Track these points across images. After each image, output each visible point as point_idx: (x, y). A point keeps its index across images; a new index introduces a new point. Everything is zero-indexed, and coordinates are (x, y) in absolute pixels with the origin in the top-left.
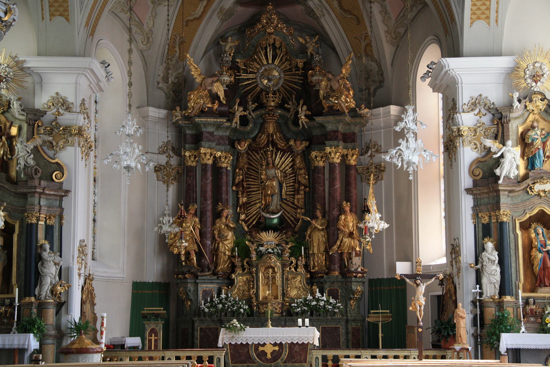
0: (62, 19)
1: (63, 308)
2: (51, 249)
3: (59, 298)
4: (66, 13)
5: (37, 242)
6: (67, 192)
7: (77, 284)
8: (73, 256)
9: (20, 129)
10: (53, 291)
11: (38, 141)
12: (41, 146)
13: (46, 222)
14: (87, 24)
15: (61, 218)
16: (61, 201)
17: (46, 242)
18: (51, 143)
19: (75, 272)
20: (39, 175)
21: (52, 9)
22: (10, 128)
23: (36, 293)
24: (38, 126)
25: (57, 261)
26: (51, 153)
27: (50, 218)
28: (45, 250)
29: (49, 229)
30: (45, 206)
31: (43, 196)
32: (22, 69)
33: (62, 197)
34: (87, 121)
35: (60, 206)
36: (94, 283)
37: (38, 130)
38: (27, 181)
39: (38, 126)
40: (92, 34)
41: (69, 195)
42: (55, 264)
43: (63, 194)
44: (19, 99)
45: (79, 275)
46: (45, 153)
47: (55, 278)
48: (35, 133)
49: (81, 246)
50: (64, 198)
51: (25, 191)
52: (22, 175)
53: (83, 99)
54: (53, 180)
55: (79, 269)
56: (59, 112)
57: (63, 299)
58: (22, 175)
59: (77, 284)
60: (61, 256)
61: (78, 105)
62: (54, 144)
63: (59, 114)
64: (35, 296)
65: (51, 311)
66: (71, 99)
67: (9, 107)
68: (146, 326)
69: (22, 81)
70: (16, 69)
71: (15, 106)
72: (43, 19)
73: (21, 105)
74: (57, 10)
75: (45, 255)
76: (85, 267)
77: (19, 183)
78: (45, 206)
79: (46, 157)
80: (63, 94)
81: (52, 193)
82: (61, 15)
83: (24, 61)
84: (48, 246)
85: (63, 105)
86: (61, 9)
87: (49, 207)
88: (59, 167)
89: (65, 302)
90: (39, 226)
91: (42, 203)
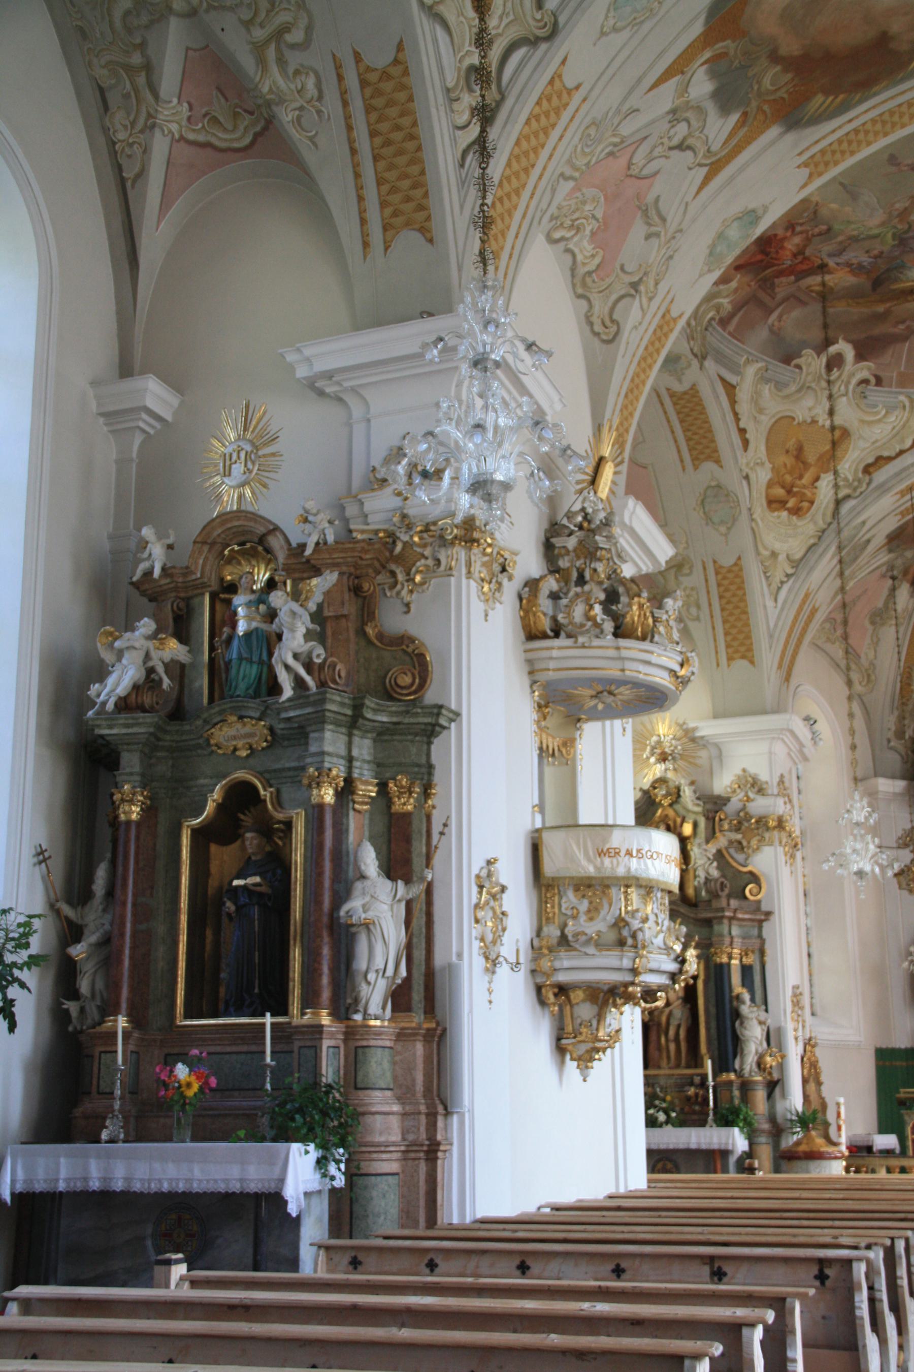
0: (745, 663)
1: (777, 1091)
2: (753, 1000)
3: (770, 1074)
4: (749, 654)
5: (731, 990)
6: (768, 914)
7: (794, 1052)
8: (785, 1011)
9: (695, 825)
10: (760, 1064)
11: (721, 841)
12: (727, 848)
14: (780, 666)
15: (762, 953)
16: (760, 928)
18: (740, 843)
19: (790, 1035)
20: (727, 891)
21: (730, 651)
22: (681, 825)
23: (737, 1066)
24: (721, 820)
25: (762, 1018)
26: (740, 857)
27: (747, 954)
28: (743, 1003)
29: (746, 970)
30: (738, 936)
31: (734, 922)
32: (693, 740)
33: (760, 922)
34: (788, 806)
35: (760, 936)
36: (818, 1051)
37: (721, 826)
38: (709, 901)
39: (721, 820)
40: (787, 679)
41: (772, 918)
42: (761, 1023)
43: (763, 917)
44: (692, 783)
45: (796, 1039)
47: (761, 1044)
48: (717, 830)
49: (795, 995)
50: (765, 924)
51: (709, 915)
52: (703, 893)
53: (782, 776)
54: (745, 898)
55: (796, 1030)
56: (748, 798)
57: (776, 1076)
58: (703, 893)
59: (794, 1052)
60: (766, 1011)
61: (775, 784)
62: (745, 843)
63: (749, 800)
64: (735, 1071)
65: (760, 1095)
66: (764, 776)
67: (679, 796)
68: (906, 1118)
69: (694, 757)
70: (685, 740)
71: (687, 793)
72: (718, 665)
73: (695, 792)
74: (737, 651)
75: (745, 1009)
76: (803, 1027)
78: (738, 936)
79: (734, 864)
80: (752, 770)
81: (747, 916)
82: (743, 657)
83: (695, 729)
84: (747, 997)
85: (753, 786)
86: (743, 649)
87: (744, 938)
88: (754, 878)
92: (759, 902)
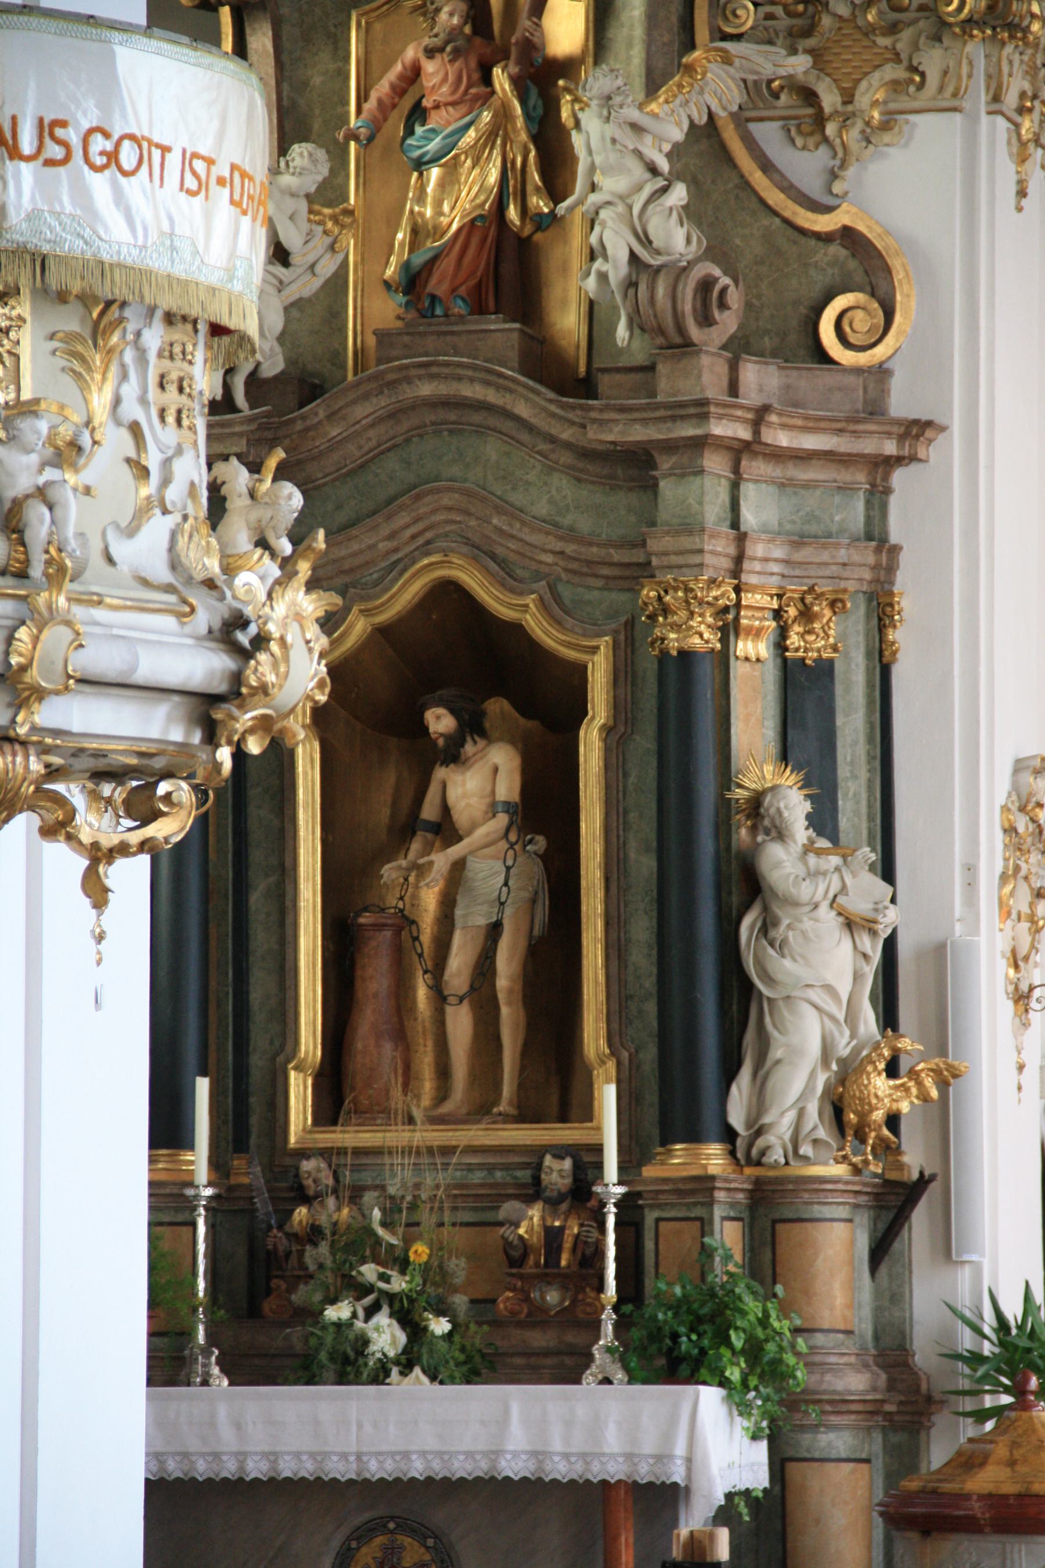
1: (920, 1218)
3: (888, 1150)
8: (971, 869)
12: (741, 119)
13: (780, 646)
17: (789, 779)
18: (809, 96)
20: (728, 322)
23: (737, 1119)
25: (859, 905)
27: (807, 615)
28: (780, 834)
30: (773, 535)
31: (753, 467)
38: (650, 368)
41: (933, 452)
42: (850, 924)
43: (890, 448)
46: (767, 166)
47: (852, 1018)
48: (702, 33)
50: (899, 477)
51: (639, 433)
52: (622, 332)
54: (823, 357)
58: (622, 332)
60: (887, 871)
62: (829, 99)
64: (729, 1135)
77: (605, 382)
78: (773, 535)
79: (775, 197)
81: (811, 442)
87: (799, 541)
89: (923, 1182)
90: (739, 671)
91: (749, 517)
92: (881, 372)
